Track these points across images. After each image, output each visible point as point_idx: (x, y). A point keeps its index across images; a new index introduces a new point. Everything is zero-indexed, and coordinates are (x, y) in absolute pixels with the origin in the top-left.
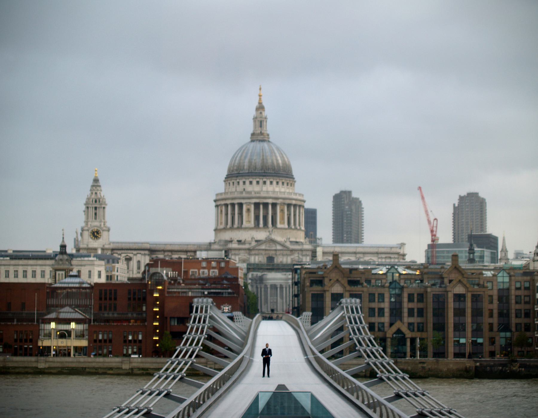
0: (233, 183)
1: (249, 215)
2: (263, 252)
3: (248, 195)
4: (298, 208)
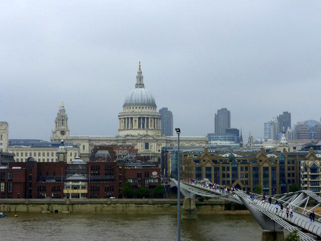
3: (135, 114)
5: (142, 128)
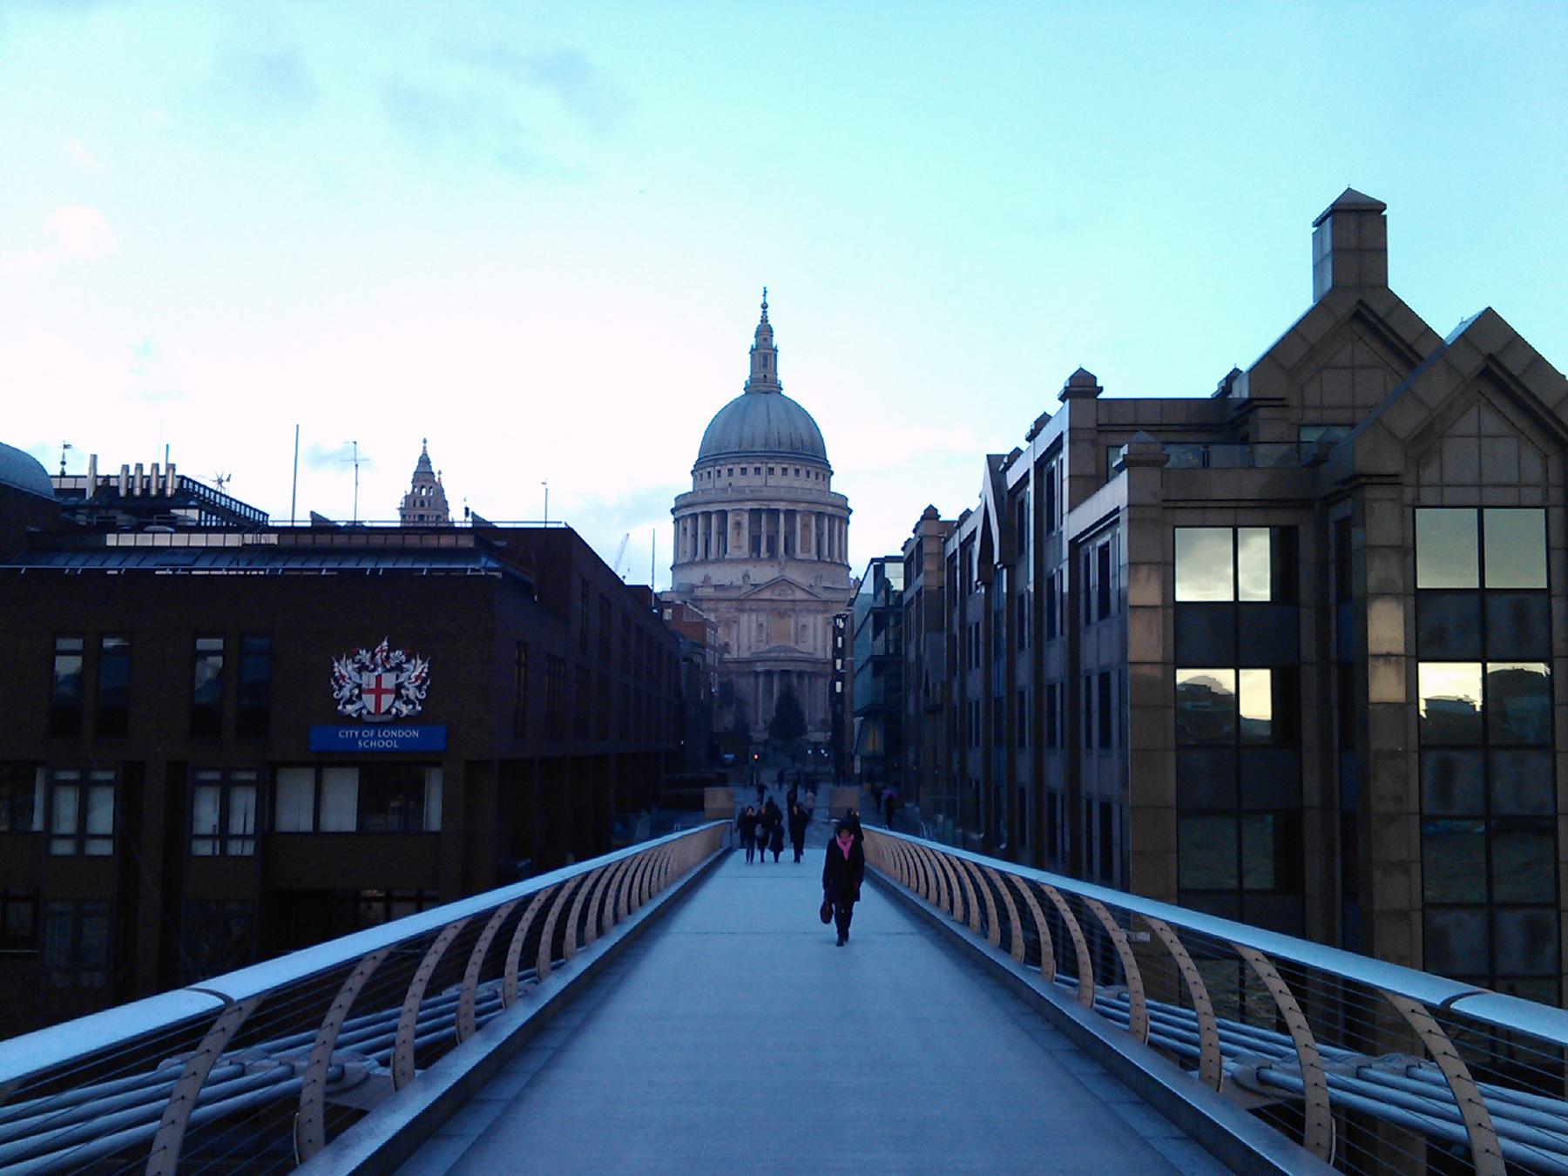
3: (735, 496)
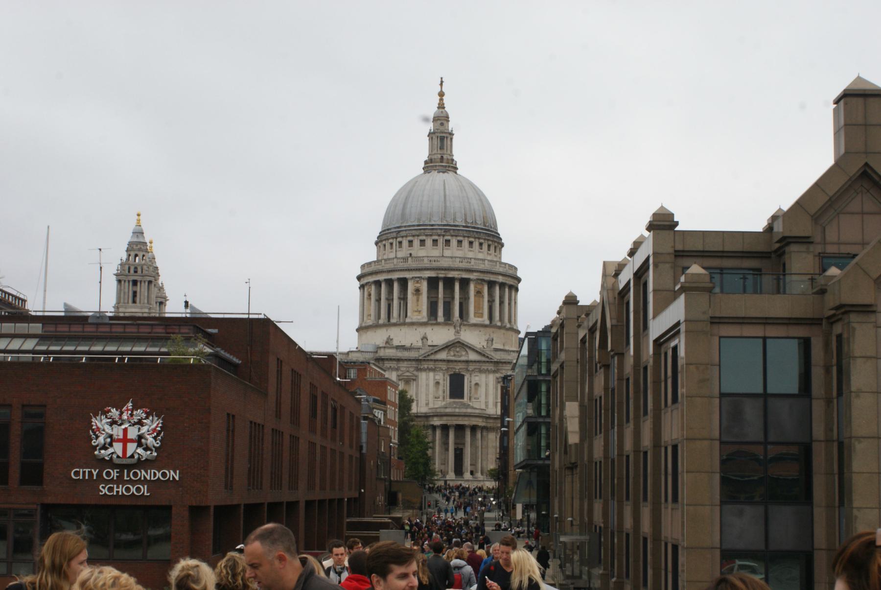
0: (391, 244)
1: (418, 300)
2: (444, 366)
4: (507, 290)
5: (441, 318)
